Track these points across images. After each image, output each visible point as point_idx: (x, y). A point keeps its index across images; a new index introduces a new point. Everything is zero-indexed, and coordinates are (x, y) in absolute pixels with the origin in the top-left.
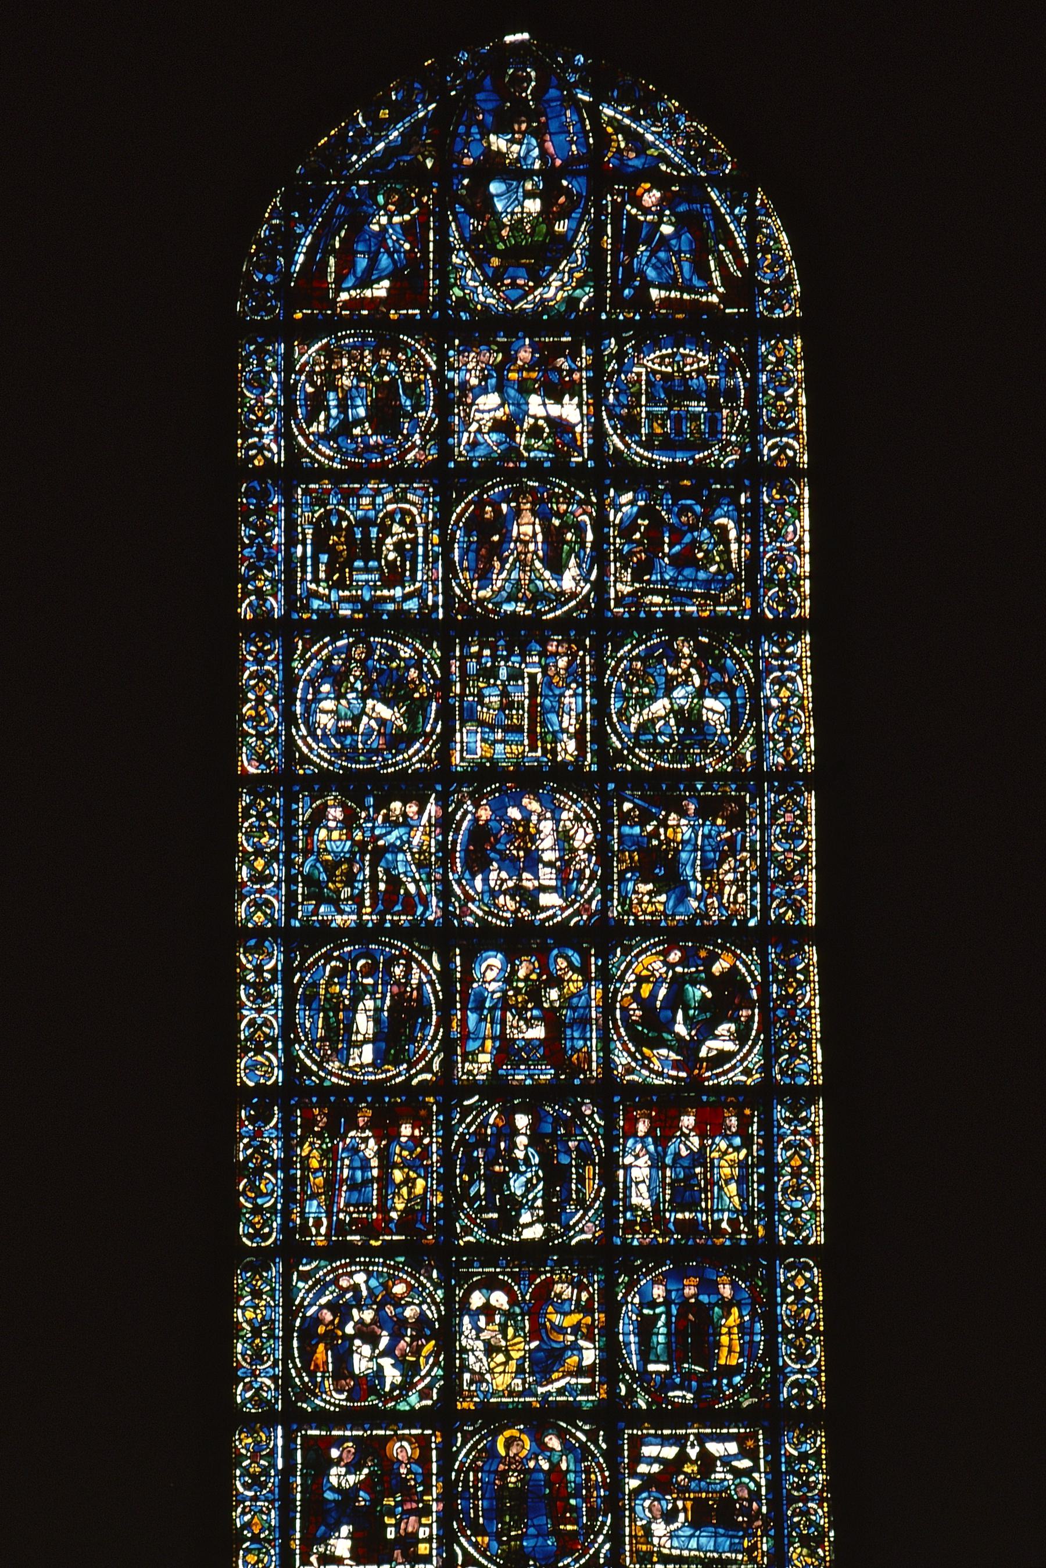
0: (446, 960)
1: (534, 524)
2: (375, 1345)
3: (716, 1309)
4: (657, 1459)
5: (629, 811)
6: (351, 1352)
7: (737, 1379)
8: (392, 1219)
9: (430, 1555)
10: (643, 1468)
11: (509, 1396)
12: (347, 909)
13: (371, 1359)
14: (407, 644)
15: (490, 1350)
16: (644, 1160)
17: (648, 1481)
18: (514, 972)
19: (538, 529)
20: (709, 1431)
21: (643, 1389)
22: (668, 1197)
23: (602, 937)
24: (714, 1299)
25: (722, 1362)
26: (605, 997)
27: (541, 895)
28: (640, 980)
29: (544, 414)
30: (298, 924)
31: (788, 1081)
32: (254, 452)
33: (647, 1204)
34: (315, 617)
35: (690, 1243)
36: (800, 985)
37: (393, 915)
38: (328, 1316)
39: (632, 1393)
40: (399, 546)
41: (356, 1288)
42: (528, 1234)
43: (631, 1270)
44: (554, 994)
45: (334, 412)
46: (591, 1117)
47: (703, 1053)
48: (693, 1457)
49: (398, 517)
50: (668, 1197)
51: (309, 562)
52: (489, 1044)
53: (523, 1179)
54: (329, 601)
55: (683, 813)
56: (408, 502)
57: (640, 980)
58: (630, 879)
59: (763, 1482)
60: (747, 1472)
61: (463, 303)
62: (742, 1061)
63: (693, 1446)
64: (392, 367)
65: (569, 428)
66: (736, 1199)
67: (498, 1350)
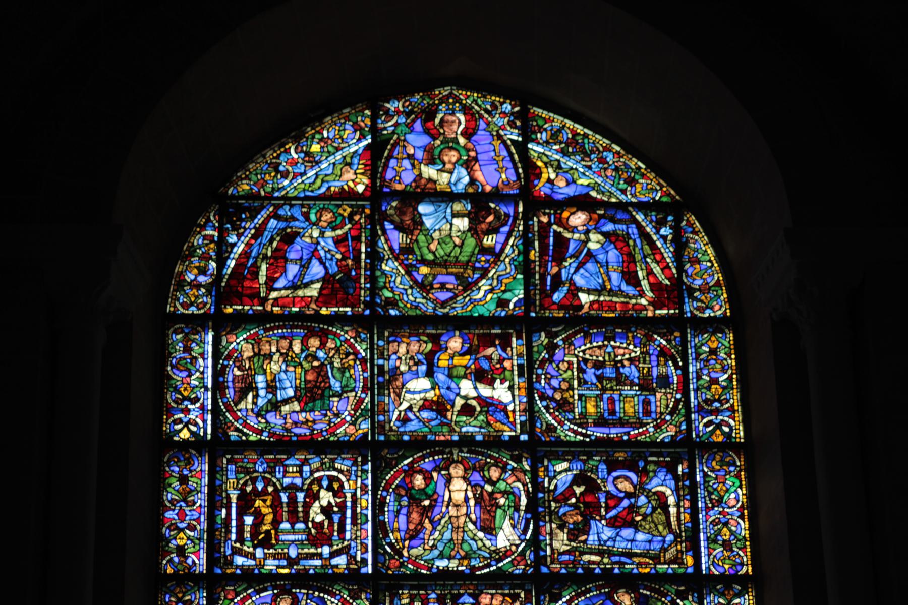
1: (466, 490)
14: (334, 595)
19: (470, 494)
29: (475, 395)
32: (179, 426)
34: (238, 571)
40: (327, 511)
45: (262, 393)
49: (325, 483)
51: (234, 523)
54: (254, 558)
56: (335, 469)
61: (392, 303)
64: (321, 354)
65: (502, 408)
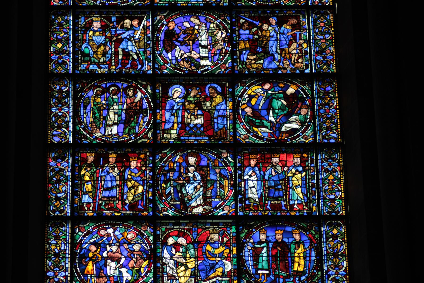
0: (154, 89)
2: (118, 262)
3: (292, 245)
5: (243, 23)
6: (105, 265)
7: (303, 278)
8: (126, 204)
12: (103, 66)
13: (116, 269)
15: (177, 264)
16: (254, 178)
18: (188, 94)
22: (266, 194)
23: (232, 80)
24: (291, 240)
25: (296, 269)
26: (233, 105)
27: (201, 61)
28: (251, 97)
30: (78, 72)
31: (326, 141)
33: (256, 197)
35: (279, 214)
36: (331, 99)
37: (126, 69)
38: (93, 248)
41: (108, 235)
42: (195, 211)
43: (249, 227)
44: (208, 104)
46: (226, 158)
47: (283, 129)
50: (266, 194)
52: (176, 125)
53: (192, 186)
55: (270, 24)
57: (251, 97)
58: (245, 54)
62: (303, 133)
66: (301, 195)
67: (182, 264)
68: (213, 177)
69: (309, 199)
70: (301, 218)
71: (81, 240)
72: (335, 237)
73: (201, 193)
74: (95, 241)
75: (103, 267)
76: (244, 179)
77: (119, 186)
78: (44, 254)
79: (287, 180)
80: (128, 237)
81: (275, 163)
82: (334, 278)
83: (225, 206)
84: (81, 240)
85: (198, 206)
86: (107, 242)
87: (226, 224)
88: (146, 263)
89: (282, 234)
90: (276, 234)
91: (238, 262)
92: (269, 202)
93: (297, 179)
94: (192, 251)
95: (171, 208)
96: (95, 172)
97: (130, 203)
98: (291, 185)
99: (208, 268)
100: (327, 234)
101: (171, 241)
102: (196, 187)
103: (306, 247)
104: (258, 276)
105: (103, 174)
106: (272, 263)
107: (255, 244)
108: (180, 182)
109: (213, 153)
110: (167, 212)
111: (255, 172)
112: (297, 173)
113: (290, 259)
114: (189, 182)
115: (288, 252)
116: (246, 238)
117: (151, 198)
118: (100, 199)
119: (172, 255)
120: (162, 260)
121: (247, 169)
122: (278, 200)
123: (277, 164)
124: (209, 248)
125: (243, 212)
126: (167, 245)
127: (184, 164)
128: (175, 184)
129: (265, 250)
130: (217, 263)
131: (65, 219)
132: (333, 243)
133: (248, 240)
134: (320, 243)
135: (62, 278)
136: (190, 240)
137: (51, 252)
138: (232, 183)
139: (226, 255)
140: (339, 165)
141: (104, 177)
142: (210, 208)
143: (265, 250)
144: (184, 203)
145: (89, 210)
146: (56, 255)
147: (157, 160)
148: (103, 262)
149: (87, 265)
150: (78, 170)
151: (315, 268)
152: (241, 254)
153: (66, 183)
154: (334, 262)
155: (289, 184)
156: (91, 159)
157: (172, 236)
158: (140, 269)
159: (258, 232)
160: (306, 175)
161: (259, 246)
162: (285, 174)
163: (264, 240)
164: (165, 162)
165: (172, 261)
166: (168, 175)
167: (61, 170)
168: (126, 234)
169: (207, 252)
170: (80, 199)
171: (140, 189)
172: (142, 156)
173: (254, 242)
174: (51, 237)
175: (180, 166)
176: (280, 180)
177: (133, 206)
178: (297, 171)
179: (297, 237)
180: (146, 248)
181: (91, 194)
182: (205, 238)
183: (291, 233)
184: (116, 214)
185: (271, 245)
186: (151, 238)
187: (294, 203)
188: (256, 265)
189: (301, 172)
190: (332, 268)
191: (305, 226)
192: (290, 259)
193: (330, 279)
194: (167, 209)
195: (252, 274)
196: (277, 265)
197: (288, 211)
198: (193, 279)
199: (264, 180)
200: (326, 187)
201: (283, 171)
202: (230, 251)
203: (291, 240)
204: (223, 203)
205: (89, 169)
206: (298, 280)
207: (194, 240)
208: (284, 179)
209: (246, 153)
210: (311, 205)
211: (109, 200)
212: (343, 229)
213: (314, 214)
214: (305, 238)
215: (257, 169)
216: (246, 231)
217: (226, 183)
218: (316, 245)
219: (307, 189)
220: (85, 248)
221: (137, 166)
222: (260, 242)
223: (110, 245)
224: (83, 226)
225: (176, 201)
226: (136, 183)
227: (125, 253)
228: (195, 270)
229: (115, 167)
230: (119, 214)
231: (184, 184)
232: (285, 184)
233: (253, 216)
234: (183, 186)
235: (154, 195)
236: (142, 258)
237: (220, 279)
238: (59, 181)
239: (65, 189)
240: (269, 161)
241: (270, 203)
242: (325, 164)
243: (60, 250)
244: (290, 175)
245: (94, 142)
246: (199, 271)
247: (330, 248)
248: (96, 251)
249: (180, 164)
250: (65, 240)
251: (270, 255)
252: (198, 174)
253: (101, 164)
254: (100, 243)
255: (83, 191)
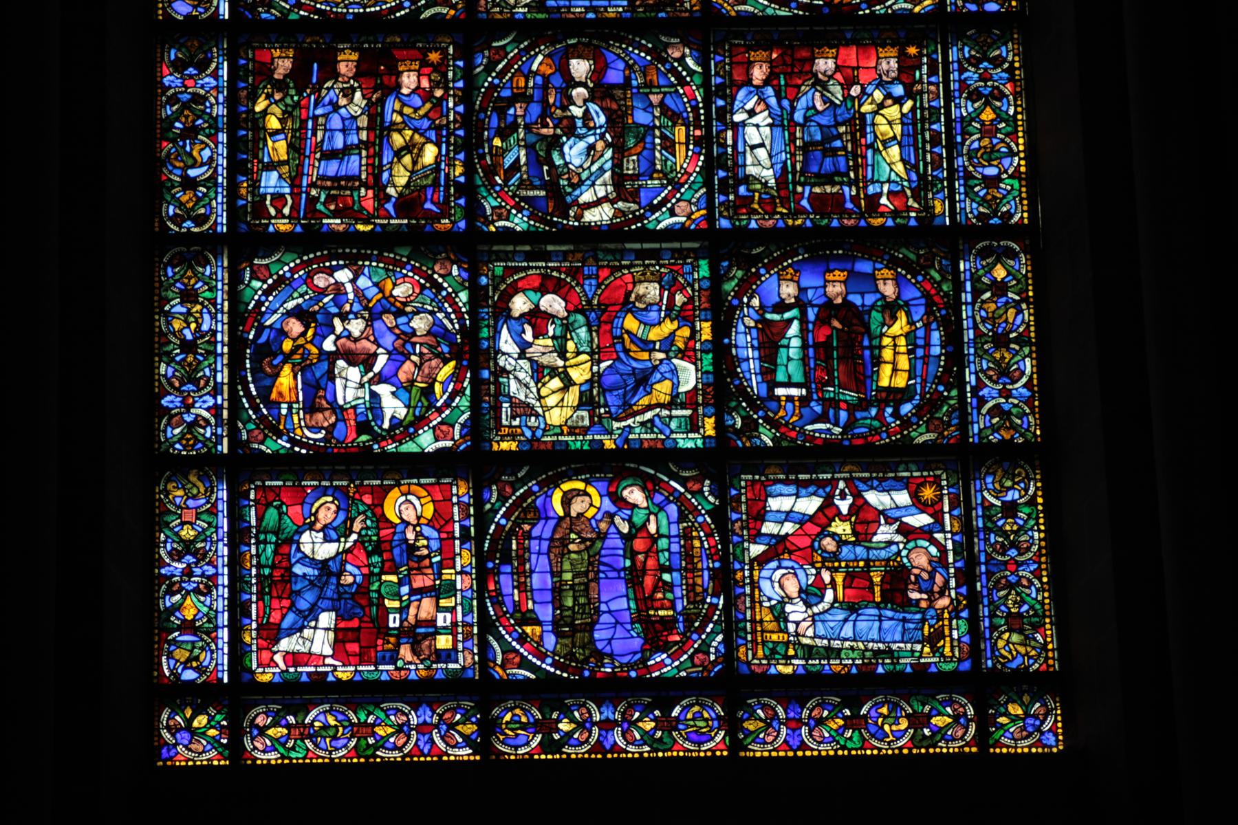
2: (369, 368)
3: (874, 313)
4: (788, 516)
6: (331, 377)
7: (906, 408)
8: (389, 197)
9: (455, 648)
10: (769, 528)
11: (569, 434)
13: (362, 386)
15: (540, 372)
16: (762, 118)
17: (778, 548)
20: (867, 475)
21: (767, 419)
24: (870, 299)
25: (884, 382)
33: (768, 174)
35: (835, 223)
38: (295, 327)
39: (750, 427)
41: (339, 286)
42: (591, 216)
43: (747, 262)
46: (681, 60)
48: (845, 511)
53: (582, 145)
59: (950, 545)
60: (926, 533)
63: (843, 496)
66: (899, 167)
67: (554, 372)
68: (642, 117)
69: (922, 177)
70: (900, 235)
71: (259, 304)
72: (999, 288)
73: (608, 165)
74: (298, 305)
75: (323, 383)
76: (732, 122)
77: (367, 145)
78: (149, 342)
79: (859, 123)
80: (395, 293)
81: (824, 74)
82: (998, 406)
83: (679, 200)
84: (259, 304)
85: (598, 203)
86: (334, 310)
87: (681, 254)
88: (448, 369)
89: (844, 282)
90: (826, 281)
91: (715, 363)
92: (807, 189)
93: (888, 122)
94: (583, 332)
95: (520, 210)
96: (297, 105)
97: (400, 194)
98: (870, 138)
99: (631, 381)
100: (975, 279)
101: (520, 304)
102: (591, 147)
103: (916, 318)
104: (774, 405)
105: (319, 112)
106: (816, 365)
107: (765, 312)
108: (544, 131)
109: (642, 48)
110: (507, 219)
111: (764, 100)
112: (889, 102)
113: (867, 353)
114: (571, 131)
115: (863, 335)
116: (738, 295)
117: (462, 179)
118: (312, 185)
119: (524, 347)
120: (495, 359)
121: (741, 94)
122: (833, 184)
123: (831, 77)
124: (631, 323)
125: (730, 218)
126: (509, 317)
127: (557, 81)
128: (532, 139)
129: (794, 329)
130: (655, 368)
131: (210, 243)
132: (993, 306)
133: (745, 300)
134: (957, 305)
135: (206, 414)
136: (576, 302)
137: (173, 339)
138: (698, 133)
139: (681, 345)
140: (1012, 79)
141: (321, 121)
142: (634, 206)
143: (794, 329)
144: (557, 193)
145: (280, 215)
146: (188, 347)
147: (478, 70)
148: (325, 366)
149: (277, 375)
150: (248, 97)
151: (940, 380)
152: (726, 341)
153: (212, 137)
154: (995, 361)
155: (864, 135)
156: (283, 66)
157: (523, 291)
158: (431, 386)
159: (775, 277)
160: (913, 109)
161: (776, 317)
162: (853, 106)
163: (793, 300)
164: (501, 75)
165: (525, 364)
166: (511, 111)
167: (198, 99)
168: (389, 285)
169: (626, 336)
170: (255, 185)
171: (430, 154)
172: (434, 57)
173: (762, 306)
174: (171, 295)
175: (545, 87)
176: (837, 124)
177: (409, 203)
178: (888, 96)
179: (889, 290)
180: (450, 326)
181: (285, 169)
182: (620, 295)
183: (872, 278)
184: (361, 227)
185: (811, 314)
186: (463, 296)
187: (879, 190)
188: (768, 374)
189: (899, 101)
190: (990, 378)
191: (912, 256)
192: (867, 353)
193: (984, 411)
194: (509, 212)
195: (759, 398)
196: (830, 371)
197: (862, 216)
198: (585, 414)
199: (793, 124)
200: (974, 142)
201: (847, 96)
202: (694, 332)
203: (870, 299)
204: (672, 194)
205: (277, 96)
206: (891, 415)
207: (589, 302)
208: (849, 122)
209: (739, 45)
210: (930, 196)
211: (340, 188)
212: (1023, 265)
213: (937, 221)
214: (911, 293)
215: (770, 91)
216: (740, 274)
217: (680, 133)
218: (944, 313)
219: (916, 150)
220: (270, 327)
221: (418, 87)
222: (781, 307)
223: (344, 317)
224: (264, 262)
225: (534, 188)
226: (417, 136)
227: (388, 340)
228: (592, 388)
229: (353, 90)
230: (369, 228)
231: (556, 138)
232: (853, 135)
233: (761, 230)
234: (555, 143)
235: (469, 171)
236: (437, 356)
237: (665, 412)
238: (191, 132)
239: (211, 155)
240: (807, 68)
241: (811, 192)
242: (971, 74)
243: (199, 333)
244: (866, 108)
245: (293, 17)
246: (604, 391)
247: (984, 320)
248: (303, 334)
249: (546, 79)
250: (213, 302)
251: (811, 343)
252: (597, 108)
253: (314, 80)
254: (315, 313)
255: (261, 161)
